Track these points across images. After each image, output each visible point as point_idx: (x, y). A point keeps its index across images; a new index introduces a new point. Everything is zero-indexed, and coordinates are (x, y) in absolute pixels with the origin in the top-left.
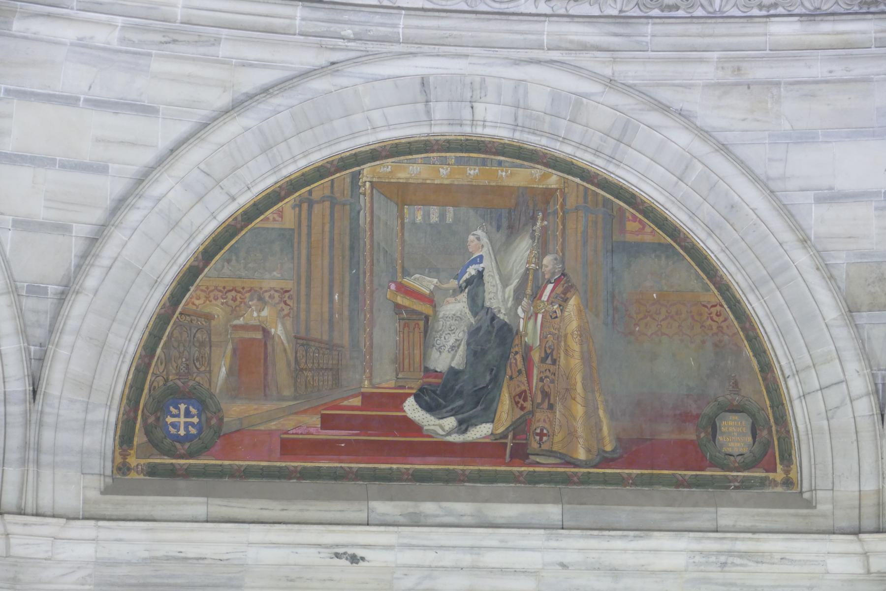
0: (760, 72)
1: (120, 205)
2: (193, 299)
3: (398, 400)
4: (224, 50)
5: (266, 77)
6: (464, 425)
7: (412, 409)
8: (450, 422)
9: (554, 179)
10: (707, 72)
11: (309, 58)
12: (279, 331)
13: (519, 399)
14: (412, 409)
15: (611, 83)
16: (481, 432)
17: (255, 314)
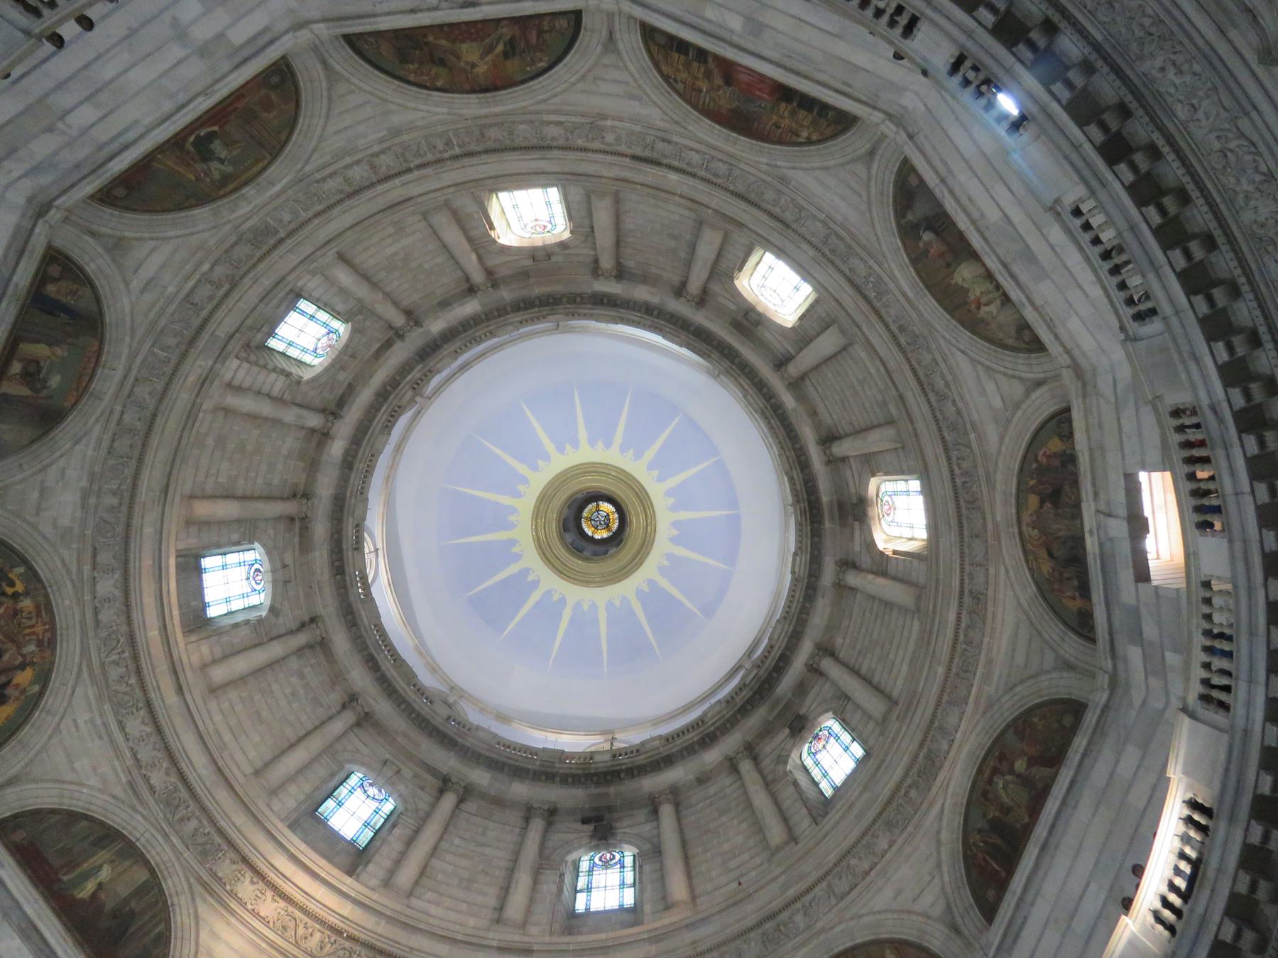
0: (199, 254)
1: (329, 110)
2: (292, 105)
3: (220, 128)
4: (329, 157)
5: (313, 159)
6: (198, 137)
7: (216, 128)
8: (202, 134)
9: (222, 193)
10: (212, 242)
11: (307, 168)
12: (265, 115)
13: (188, 152)
14: (216, 128)
15: (229, 221)
16: (192, 138)
17: (275, 113)
